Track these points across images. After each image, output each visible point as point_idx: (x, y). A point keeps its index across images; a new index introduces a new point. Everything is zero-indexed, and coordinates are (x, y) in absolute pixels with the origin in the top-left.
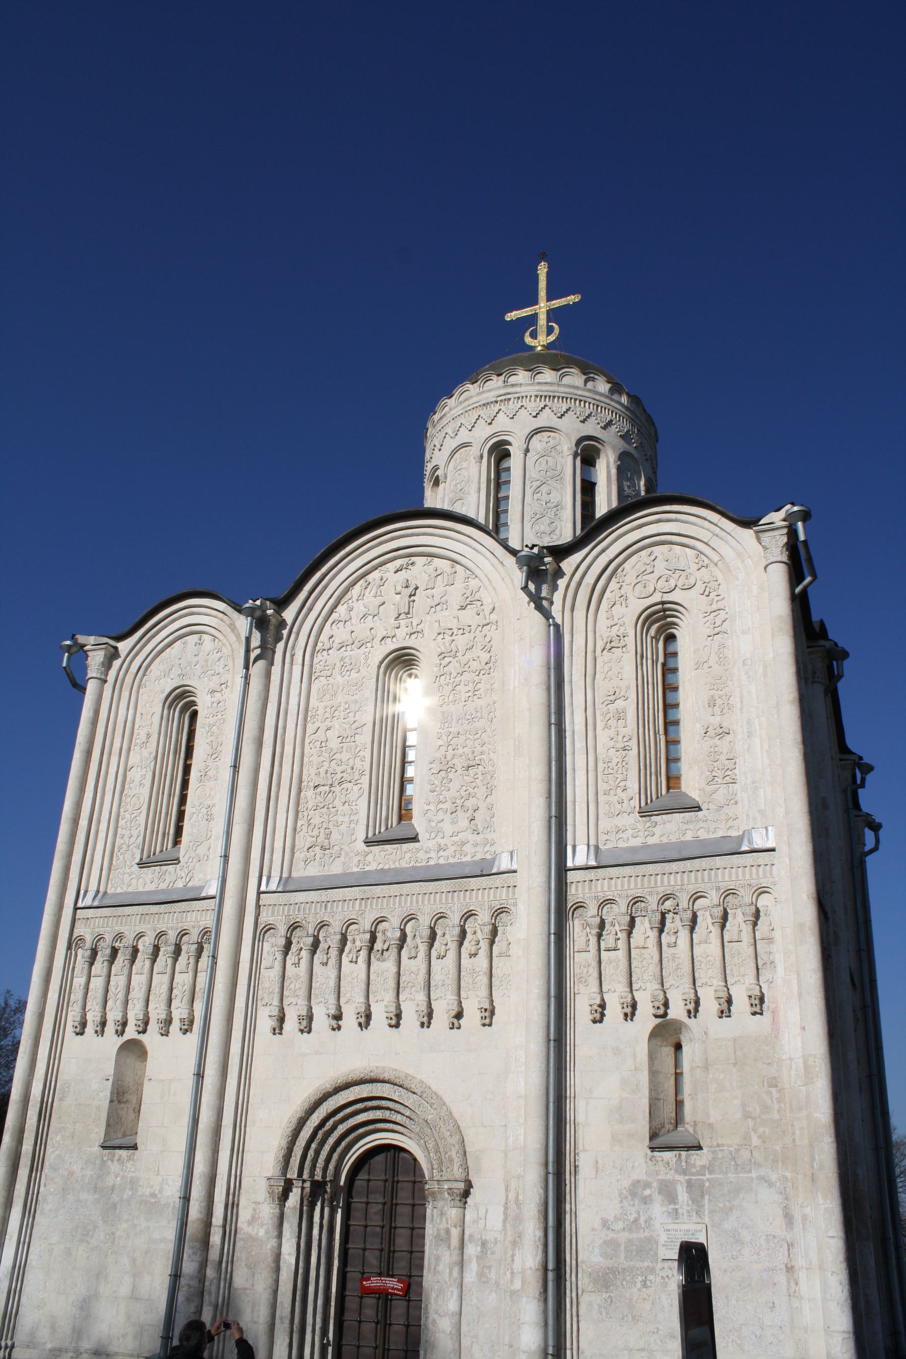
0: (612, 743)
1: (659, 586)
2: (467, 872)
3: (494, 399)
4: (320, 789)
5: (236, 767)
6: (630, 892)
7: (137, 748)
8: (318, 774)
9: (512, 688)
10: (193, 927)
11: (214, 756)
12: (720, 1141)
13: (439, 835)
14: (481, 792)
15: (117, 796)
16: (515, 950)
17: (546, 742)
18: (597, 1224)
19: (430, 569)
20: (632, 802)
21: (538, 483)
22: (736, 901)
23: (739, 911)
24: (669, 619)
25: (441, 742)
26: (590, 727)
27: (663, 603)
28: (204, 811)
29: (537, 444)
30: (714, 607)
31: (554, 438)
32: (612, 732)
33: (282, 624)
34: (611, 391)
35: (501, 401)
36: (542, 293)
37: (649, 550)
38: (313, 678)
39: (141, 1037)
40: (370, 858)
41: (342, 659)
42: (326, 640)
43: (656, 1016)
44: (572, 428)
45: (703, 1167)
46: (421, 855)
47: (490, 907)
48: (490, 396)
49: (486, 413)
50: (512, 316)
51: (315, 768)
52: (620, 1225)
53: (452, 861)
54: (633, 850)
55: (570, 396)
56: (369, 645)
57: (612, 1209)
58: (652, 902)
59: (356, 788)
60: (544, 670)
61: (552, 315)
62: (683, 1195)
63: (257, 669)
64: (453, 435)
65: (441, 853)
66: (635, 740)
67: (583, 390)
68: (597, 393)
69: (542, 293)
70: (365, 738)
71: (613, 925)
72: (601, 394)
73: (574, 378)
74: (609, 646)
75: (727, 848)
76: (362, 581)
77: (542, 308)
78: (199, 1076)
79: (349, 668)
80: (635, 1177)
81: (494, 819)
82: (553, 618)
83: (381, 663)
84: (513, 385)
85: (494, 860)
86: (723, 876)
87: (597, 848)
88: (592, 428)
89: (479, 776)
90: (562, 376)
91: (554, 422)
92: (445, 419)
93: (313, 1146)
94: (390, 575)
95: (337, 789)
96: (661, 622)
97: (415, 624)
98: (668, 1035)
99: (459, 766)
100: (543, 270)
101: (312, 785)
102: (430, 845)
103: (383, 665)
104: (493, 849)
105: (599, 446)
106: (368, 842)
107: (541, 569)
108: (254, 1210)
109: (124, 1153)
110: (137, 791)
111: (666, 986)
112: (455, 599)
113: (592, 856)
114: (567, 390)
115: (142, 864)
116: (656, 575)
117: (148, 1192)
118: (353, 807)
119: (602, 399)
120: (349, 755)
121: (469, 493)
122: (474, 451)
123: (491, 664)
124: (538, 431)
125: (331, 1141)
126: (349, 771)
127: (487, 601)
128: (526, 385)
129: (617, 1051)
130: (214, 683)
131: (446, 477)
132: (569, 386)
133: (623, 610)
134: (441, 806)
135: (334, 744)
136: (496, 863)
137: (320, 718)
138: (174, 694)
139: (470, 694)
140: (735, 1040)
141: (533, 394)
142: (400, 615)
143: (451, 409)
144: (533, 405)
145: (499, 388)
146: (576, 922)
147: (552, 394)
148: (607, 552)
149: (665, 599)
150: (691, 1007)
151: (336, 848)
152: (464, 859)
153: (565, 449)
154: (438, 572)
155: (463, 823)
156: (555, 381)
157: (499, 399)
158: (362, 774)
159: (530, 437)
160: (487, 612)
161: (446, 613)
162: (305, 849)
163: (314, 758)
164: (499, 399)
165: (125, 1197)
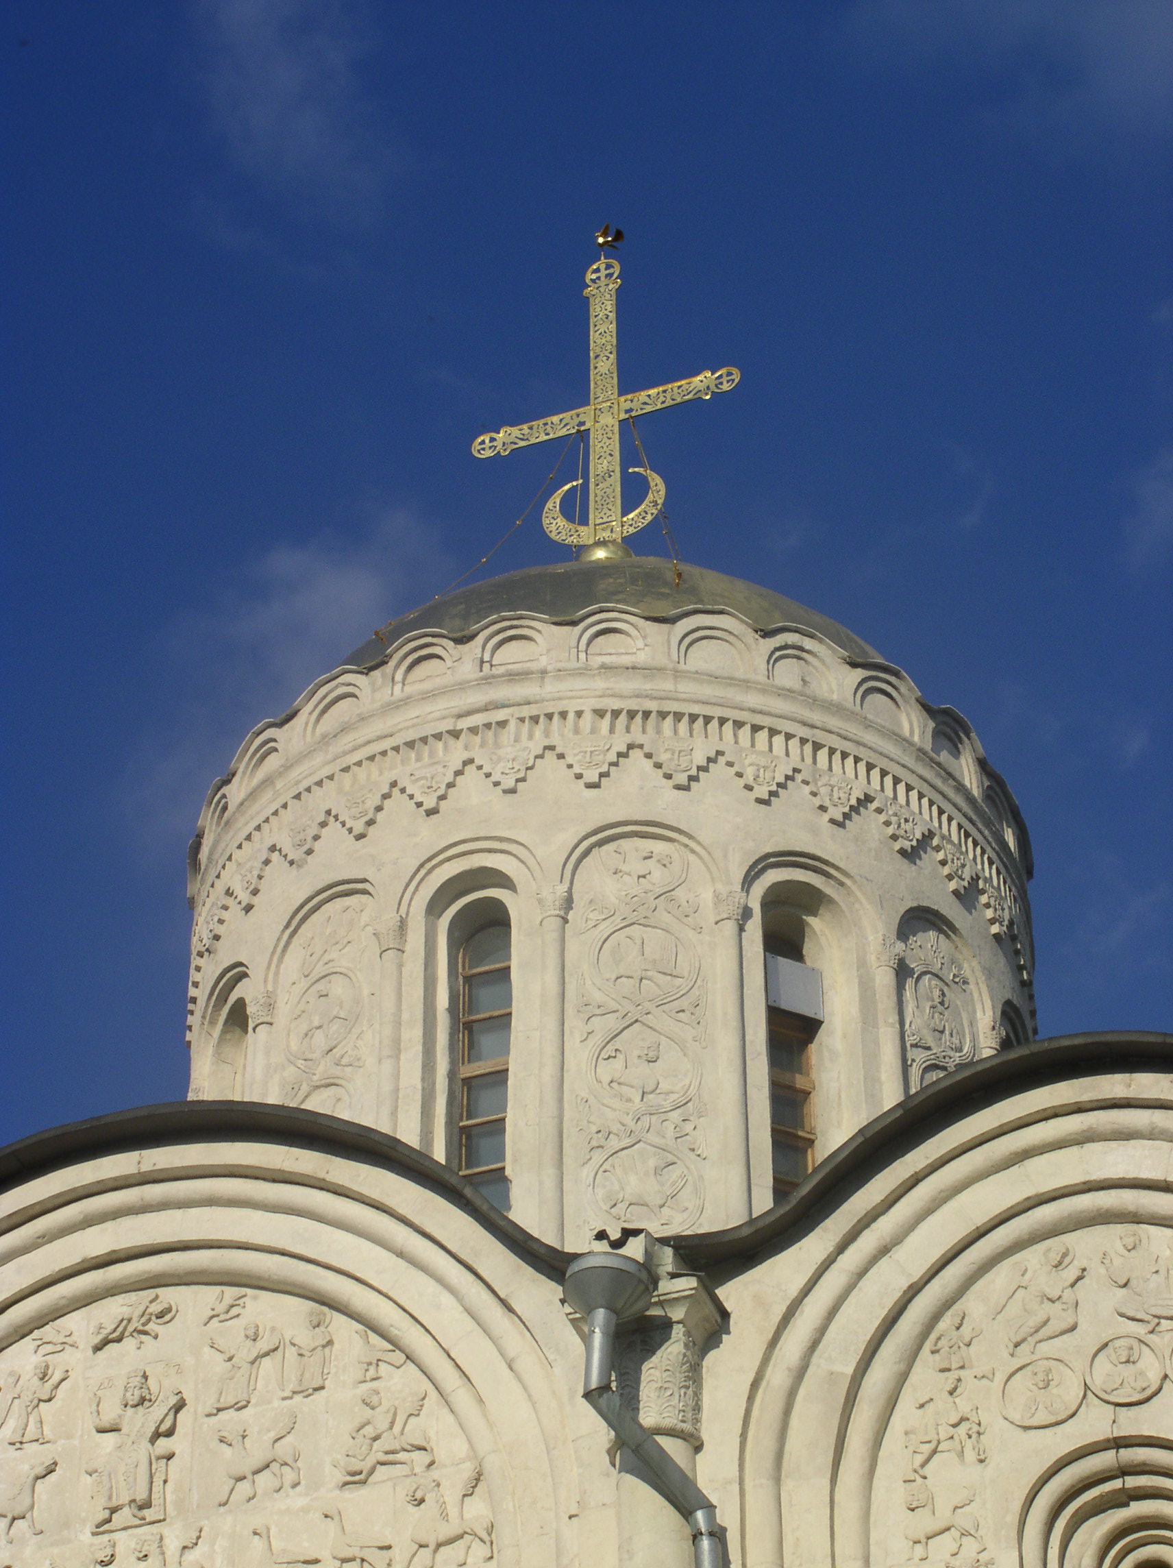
1: (1097, 1382)
3: (444, 726)
21: (613, 1023)
24: (1139, 1508)
27: (1119, 1443)
34: (866, 691)
35: (473, 730)
37: (1055, 1245)
44: (729, 829)
48: (435, 715)
49: (420, 774)
55: (717, 712)
61: (639, 436)
67: (764, 691)
68: (815, 702)
77: (604, 415)
82: (710, 1507)
84: (514, 677)
88: (796, 825)
90: (692, 640)
91: (666, 804)
94: (75, 1359)
97: (172, 1546)
100: (602, 288)
114: (708, 691)
116: (1087, 1337)
119: (834, 722)
127: (450, 1447)
131: (270, 1006)
132: (714, 678)
141: (587, 705)
142: (114, 1510)
143: (287, 767)
145: (462, 686)
147: (652, 706)
148: (899, 1253)
153: (707, 896)
154: (263, 1345)
156: (661, 660)
157: (464, 724)
160: (451, 1494)
161: (296, 1500)
164: (464, 724)
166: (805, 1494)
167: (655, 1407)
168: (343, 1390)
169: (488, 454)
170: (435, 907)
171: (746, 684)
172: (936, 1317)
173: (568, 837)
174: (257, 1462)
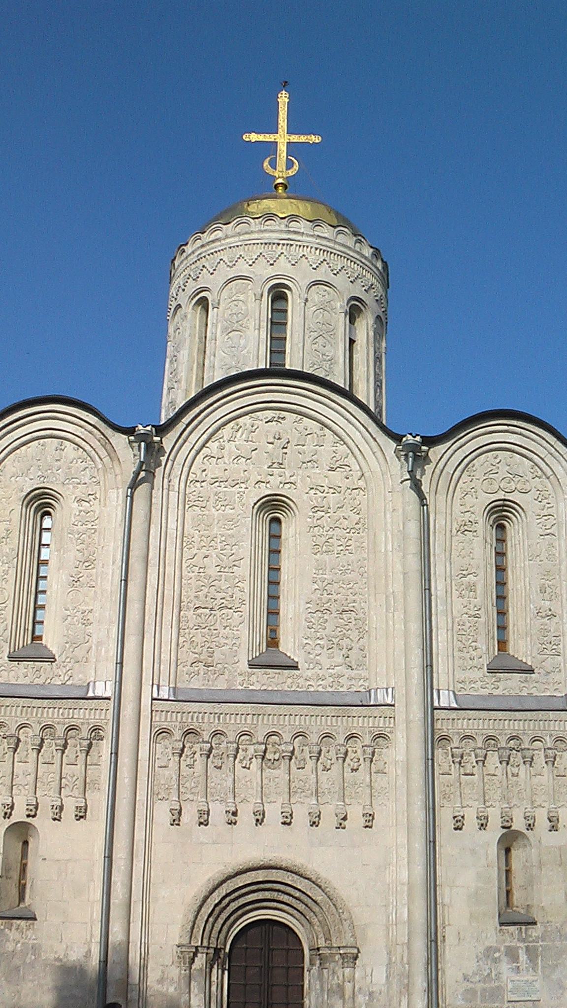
0: (465, 610)
4: (200, 611)
10: (82, 724)
11: (86, 564)
12: (550, 919)
13: (317, 668)
14: (354, 635)
16: (390, 769)
18: (460, 978)
19: (301, 427)
21: (316, 334)
26: (449, 595)
27: (505, 500)
29: (316, 295)
30: (545, 512)
33: (161, 450)
35: (283, 245)
38: (187, 506)
39: (29, 820)
40: (253, 679)
41: (216, 494)
42: (199, 473)
43: (503, 827)
45: (537, 937)
51: (194, 590)
52: (478, 978)
56: (242, 485)
57: (470, 966)
62: (523, 957)
63: (143, 489)
65: (320, 682)
69: (283, 123)
70: (243, 570)
72: (366, 258)
76: (232, 424)
78: (109, 858)
79: (226, 503)
80: (487, 944)
83: (255, 504)
84: (295, 233)
90: (339, 233)
91: (331, 278)
93: (211, 919)
96: (500, 514)
97: (288, 475)
98: (509, 841)
99: (333, 609)
101: (191, 605)
102: (310, 675)
103: (256, 506)
105: (362, 308)
106: (252, 666)
108: (163, 972)
109: (23, 923)
112: (325, 460)
115: (12, 658)
117: (52, 956)
118: (235, 633)
123: (360, 526)
124: (317, 283)
125: (224, 916)
128: (308, 235)
129: (473, 852)
130: (80, 491)
134: (319, 642)
135: (213, 571)
137: (196, 545)
138: (33, 494)
139: (341, 548)
140: (560, 848)
143: (227, 237)
149: (507, 498)
152: (341, 689)
155: (340, 660)
158: (242, 602)
159: (309, 288)
161: (317, 471)
163: (193, 581)
164: (282, 242)
165: (28, 961)
166: (441, 497)
168: (328, 447)
169: (247, 140)
174: (308, 459)
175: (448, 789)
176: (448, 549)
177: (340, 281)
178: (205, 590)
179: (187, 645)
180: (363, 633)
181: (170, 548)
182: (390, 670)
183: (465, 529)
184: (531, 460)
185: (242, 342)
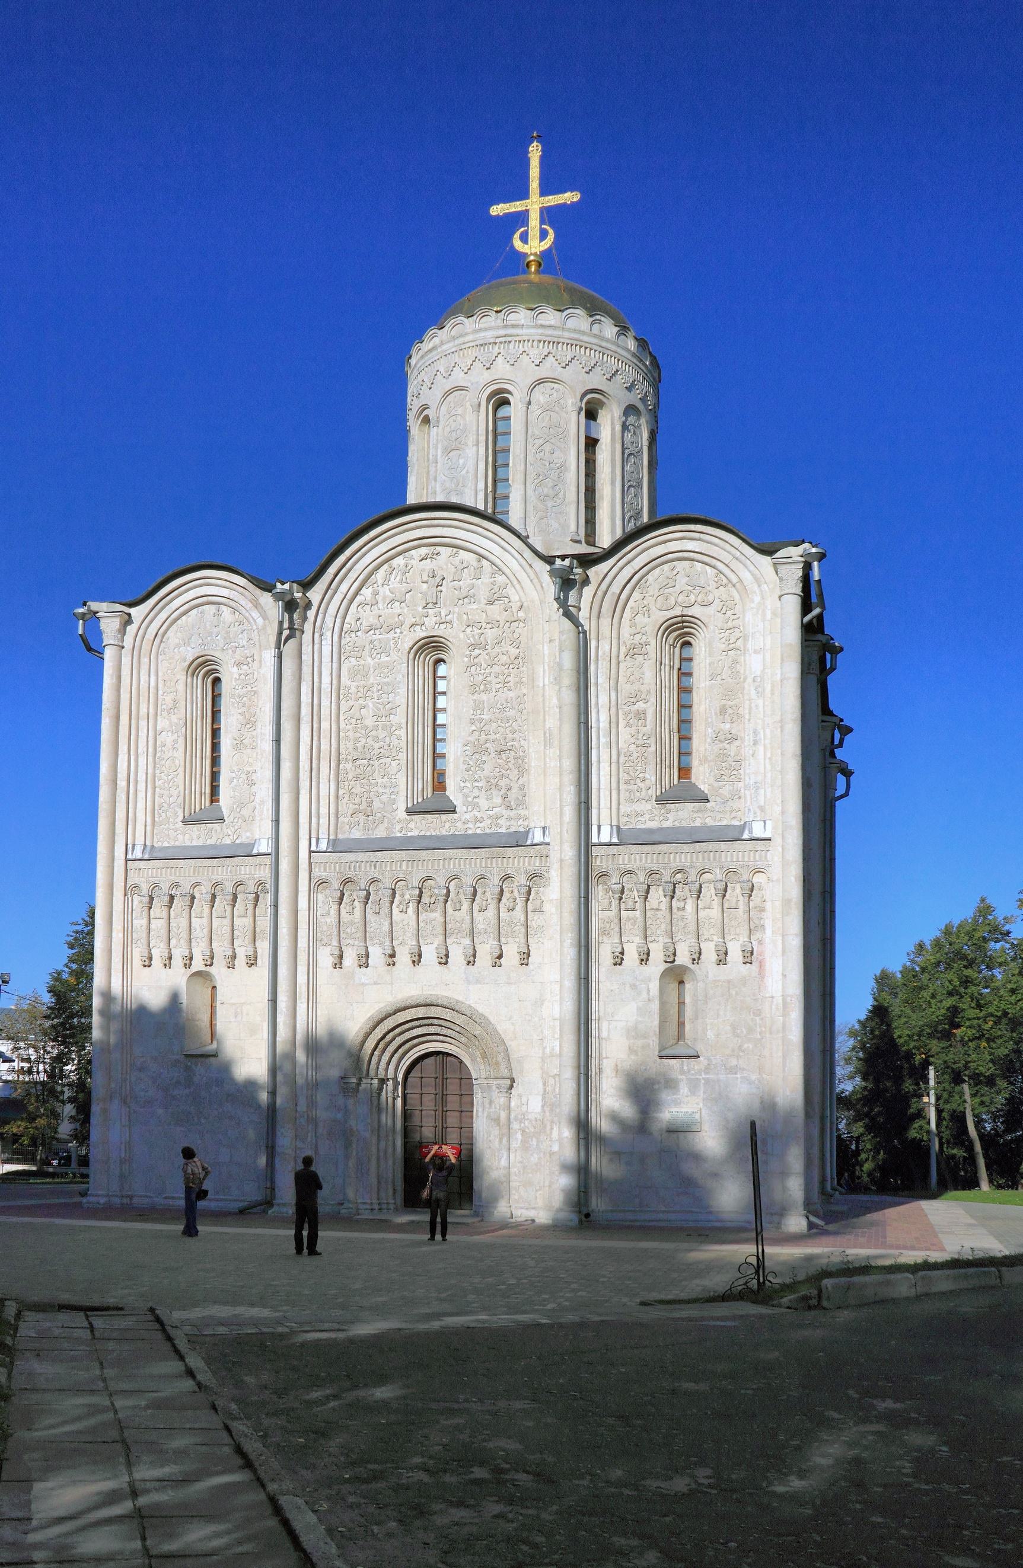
0: (633, 740)
2: (503, 841)
3: (492, 340)
4: (359, 762)
5: (278, 741)
6: (648, 866)
7: (165, 714)
8: (355, 749)
9: (541, 685)
11: (248, 726)
13: (474, 810)
14: (514, 774)
15: (150, 759)
17: (576, 737)
20: (650, 791)
21: (541, 441)
22: (736, 878)
23: (738, 886)
25: (474, 728)
26: (613, 725)
28: (244, 776)
29: (540, 396)
31: (558, 391)
32: (633, 731)
35: (501, 343)
36: (534, 185)
40: (412, 825)
46: (459, 825)
47: (526, 872)
48: (489, 335)
50: (497, 210)
53: (488, 831)
54: (650, 831)
55: (575, 342)
58: (667, 876)
59: (394, 764)
60: (574, 673)
64: (446, 375)
65: (478, 825)
66: (653, 739)
68: (602, 338)
69: (534, 185)
71: (631, 890)
72: (608, 340)
73: (579, 320)
74: (634, 652)
75: (730, 836)
77: (534, 204)
81: (526, 798)
84: (513, 326)
85: (528, 832)
86: (726, 857)
87: (618, 827)
88: (596, 381)
89: (511, 760)
90: (568, 317)
91: (559, 372)
92: (434, 353)
95: (376, 763)
100: (535, 152)
101: (349, 757)
104: (526, 823)
105: (604, 400)
106: (410, 812)
107: (571, 574)
110: (170, 754)
111: (675, 940)
113: (615, 835)
114: (573, 335)
119: (609, 345)
120: (385, 734)
121: (466, 444)
122: (470, 398)
124: (541, 381)
126: (386, 747)
128: (529, 327)
131: (438, 421)
133: (647, 620)
136: (530, 836)
143: (442, 344)
144: (536, 352)
145: (498, 328)
146: (600, 887)
147: (556, 340)
148: (632, 564)
150: (696, 956)
151: (378, 815)
152: (500, 831)
153: (570, 402)
155: (498, 800)
156: (559, 324)
157: (498, 340)
162: (349, 815)
163: (350, 734)
164: (498, 340)
166: (605, 622)
167: (571, 601)
169: (494, 214)
170: (488, 400)
171: (584, 333)
172: (640, 580)
173: (529, 381)
175: (608, 925)
176: (613, 676)
177: (565, 374)
178: (363, 741)
179: (347, 797)
180: (522, 771)
181: (325, 703)
182: (548, 811)
183: (634, 652)
184: (714, 567)
185: (461, 461)
